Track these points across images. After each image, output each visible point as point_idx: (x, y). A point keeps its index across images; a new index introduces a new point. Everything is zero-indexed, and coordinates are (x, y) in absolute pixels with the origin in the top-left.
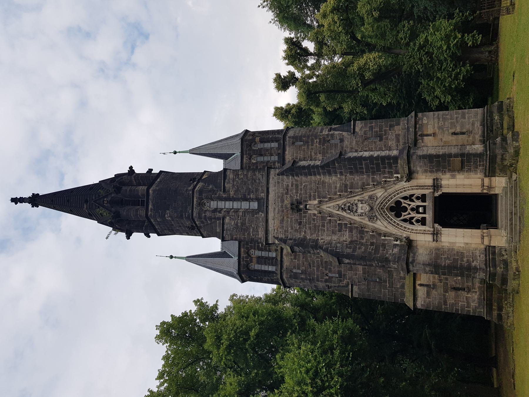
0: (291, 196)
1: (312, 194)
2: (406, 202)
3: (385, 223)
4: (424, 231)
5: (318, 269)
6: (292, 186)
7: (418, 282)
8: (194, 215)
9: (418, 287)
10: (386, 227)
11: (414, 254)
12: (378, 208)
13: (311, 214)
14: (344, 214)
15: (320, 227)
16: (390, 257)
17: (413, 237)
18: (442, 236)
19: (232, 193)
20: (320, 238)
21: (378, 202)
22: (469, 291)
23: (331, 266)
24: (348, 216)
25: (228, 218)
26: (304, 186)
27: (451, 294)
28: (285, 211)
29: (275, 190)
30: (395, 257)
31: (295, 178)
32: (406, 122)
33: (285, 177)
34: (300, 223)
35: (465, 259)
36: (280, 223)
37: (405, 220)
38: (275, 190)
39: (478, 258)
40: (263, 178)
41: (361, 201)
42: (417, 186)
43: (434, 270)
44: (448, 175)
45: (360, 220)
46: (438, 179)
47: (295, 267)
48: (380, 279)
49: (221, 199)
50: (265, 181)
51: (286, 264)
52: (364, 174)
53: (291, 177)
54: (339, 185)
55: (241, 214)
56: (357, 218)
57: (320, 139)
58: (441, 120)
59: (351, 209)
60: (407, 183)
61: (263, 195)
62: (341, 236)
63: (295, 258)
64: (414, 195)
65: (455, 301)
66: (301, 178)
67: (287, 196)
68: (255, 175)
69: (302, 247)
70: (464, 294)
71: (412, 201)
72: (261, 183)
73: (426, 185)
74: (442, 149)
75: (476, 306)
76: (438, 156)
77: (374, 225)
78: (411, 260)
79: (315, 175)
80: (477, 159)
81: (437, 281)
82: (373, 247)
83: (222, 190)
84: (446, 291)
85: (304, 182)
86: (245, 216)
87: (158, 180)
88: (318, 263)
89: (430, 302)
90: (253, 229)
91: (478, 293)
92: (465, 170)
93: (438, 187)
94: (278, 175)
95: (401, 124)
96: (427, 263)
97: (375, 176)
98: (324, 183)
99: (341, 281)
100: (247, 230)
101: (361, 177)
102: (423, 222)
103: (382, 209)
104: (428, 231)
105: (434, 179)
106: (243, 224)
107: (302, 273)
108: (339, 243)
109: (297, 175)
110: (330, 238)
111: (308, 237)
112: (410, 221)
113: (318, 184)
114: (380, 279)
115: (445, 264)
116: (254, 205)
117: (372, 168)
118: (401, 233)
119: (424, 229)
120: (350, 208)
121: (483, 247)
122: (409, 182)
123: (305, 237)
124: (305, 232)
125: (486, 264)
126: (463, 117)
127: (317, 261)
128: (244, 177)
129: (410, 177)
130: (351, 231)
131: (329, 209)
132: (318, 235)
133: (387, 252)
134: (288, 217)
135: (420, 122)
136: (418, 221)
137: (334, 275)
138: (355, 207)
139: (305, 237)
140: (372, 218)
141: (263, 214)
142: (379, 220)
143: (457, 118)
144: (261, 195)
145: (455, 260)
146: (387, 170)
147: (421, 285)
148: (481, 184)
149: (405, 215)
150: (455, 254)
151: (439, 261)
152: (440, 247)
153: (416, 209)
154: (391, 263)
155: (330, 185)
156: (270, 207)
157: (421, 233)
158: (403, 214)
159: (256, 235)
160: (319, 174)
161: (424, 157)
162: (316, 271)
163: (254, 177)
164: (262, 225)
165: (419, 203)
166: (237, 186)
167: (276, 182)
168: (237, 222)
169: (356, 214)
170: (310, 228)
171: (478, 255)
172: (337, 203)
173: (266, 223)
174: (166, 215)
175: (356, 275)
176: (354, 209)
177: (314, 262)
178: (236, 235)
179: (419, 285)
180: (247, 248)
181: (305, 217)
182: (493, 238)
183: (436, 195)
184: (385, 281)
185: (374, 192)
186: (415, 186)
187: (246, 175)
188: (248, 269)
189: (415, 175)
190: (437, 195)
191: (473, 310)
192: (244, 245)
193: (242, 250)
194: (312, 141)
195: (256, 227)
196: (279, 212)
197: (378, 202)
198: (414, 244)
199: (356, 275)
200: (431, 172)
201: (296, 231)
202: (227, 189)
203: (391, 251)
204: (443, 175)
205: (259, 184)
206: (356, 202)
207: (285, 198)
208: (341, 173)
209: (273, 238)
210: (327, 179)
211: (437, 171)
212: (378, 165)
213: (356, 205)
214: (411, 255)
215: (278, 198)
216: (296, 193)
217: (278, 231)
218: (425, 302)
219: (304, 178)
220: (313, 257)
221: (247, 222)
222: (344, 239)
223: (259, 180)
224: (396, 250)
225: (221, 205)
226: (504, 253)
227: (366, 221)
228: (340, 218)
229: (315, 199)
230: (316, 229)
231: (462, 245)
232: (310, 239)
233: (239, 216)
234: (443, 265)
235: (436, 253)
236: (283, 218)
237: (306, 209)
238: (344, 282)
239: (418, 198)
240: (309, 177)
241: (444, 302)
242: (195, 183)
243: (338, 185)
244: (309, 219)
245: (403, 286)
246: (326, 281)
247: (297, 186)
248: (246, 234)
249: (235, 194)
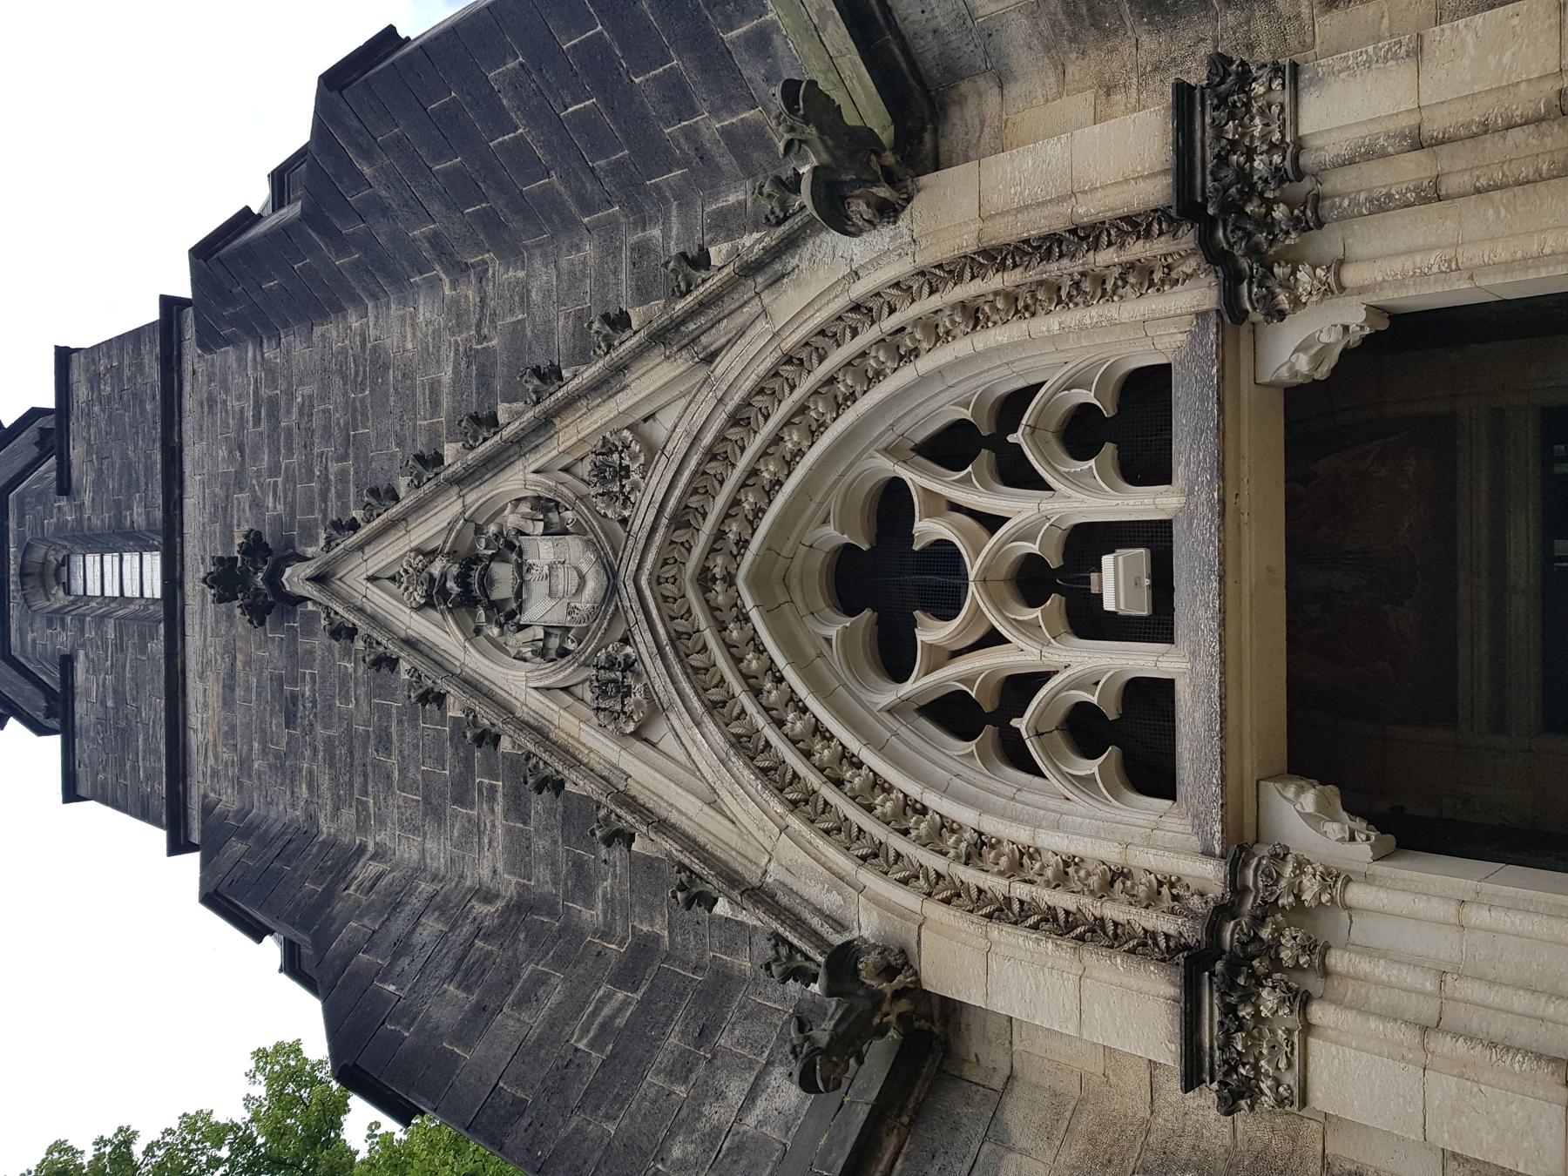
2: (947, 486)
4: (1114, 878)
12: (656, 581)
18: (1317, 1012)
46: (1245, 78)
54: (450, 370)
60: (880, 238)
71: (1018, 474)
73: (1088, 209)
82: (626, 1003)
97: (656, 232)
103: (705, 579)
104: (1165, 891)
105: (1184, 98)
119: (1103, 851)
122: (887, 211)
138: (503, 573)
157: (1050, 915)
158: (931, 633)
169: (516, 640)
190: (1303, 364)
198: (985, 1054)
203: (735, 1091)
243: (447, 375)
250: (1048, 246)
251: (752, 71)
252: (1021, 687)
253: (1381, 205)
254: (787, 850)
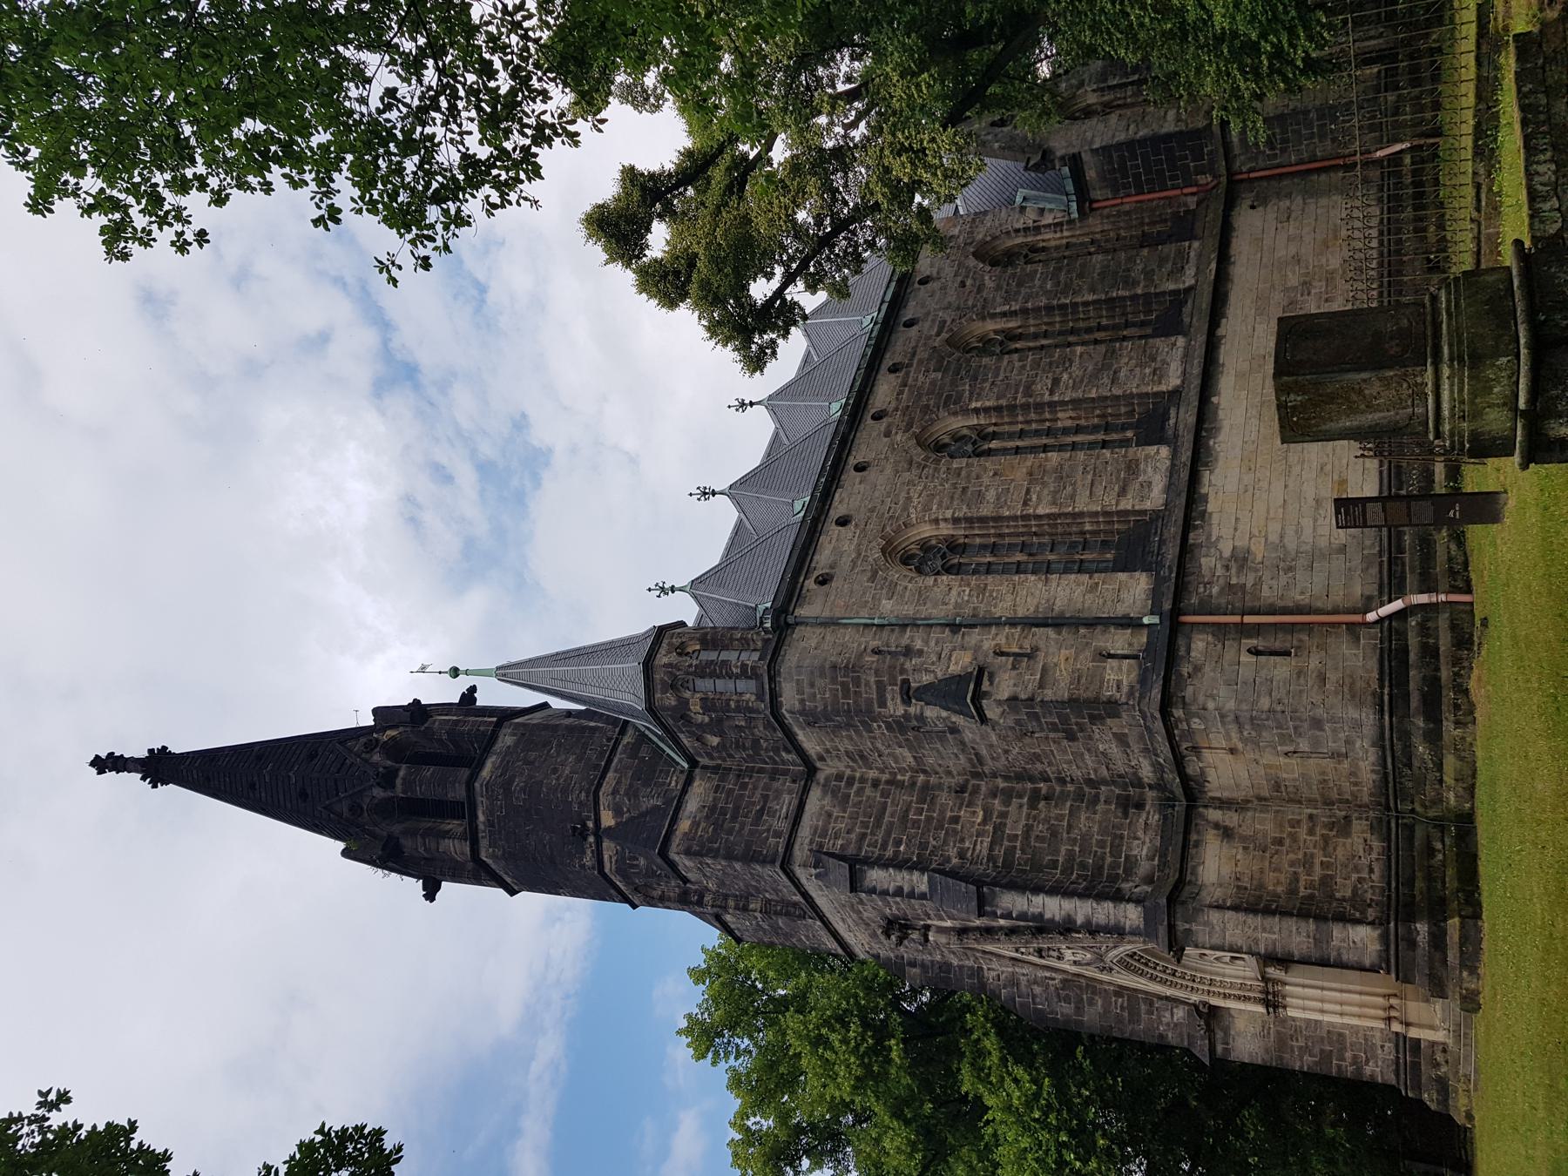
11: (1226, 1031)
16: (1170, 1035)
30: (1181, 1035)
74: (1264, 930)
87: (481, 818)
115: (1302, 1067)
133: (1159, 1017)
145: (1326, 1057)
150: (1322, 1038)
151: (1287, 1056)
171: (1379, 1043)
203: (1168, 1014)
214: (1219, 1035)
235: (1278, 1032)
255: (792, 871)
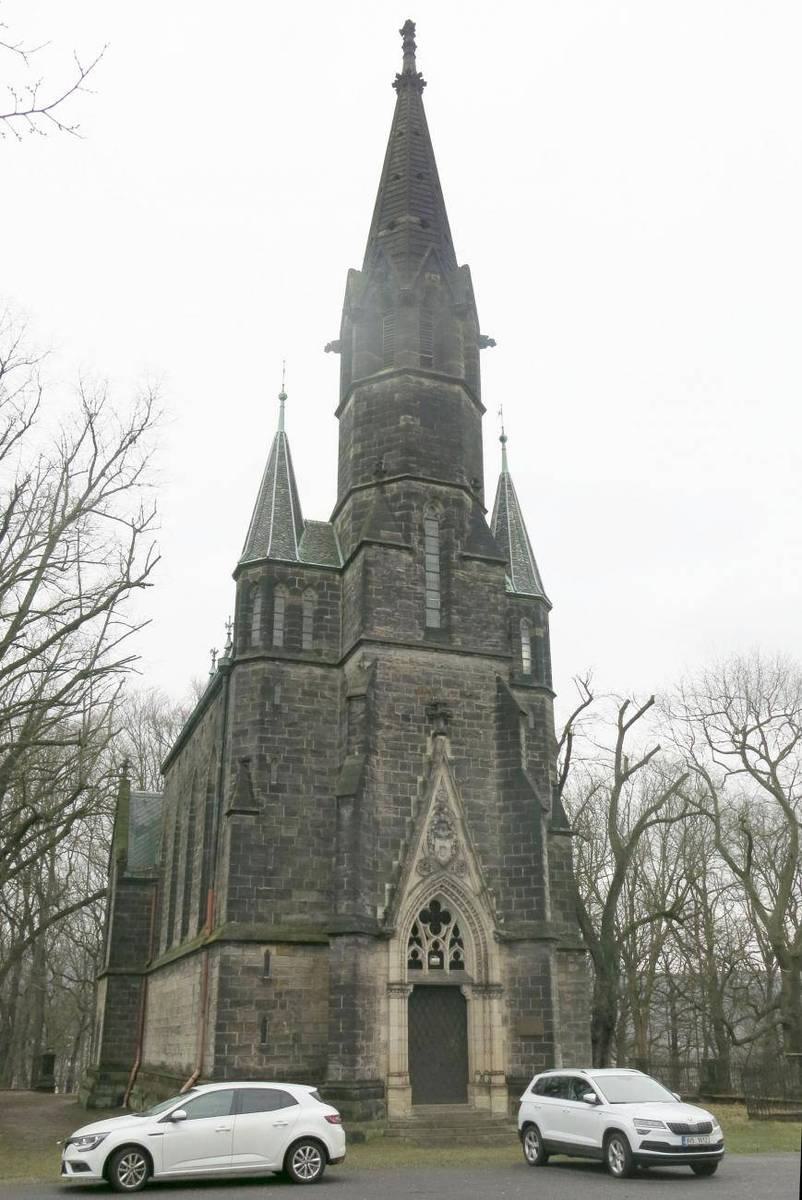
0: (458, 702)
1: (464, 748)
3: (418, 892)
5: (286, 741)
6: (478, 707)
7: (273, 950)
8: (413, 482)
9: (263, 949)
10: (410, 894)
11: (367, 947)
13: (426, 742)
14: (431, 813)
15: (400, 761)
17: (394, 945)
19: (459, 574)
20: (378, 758)
21: (454, 878)
22: (262, 1050)
23: (293, 772)
24: (428, 821)
25: (411, 559)
26: (478, 733)
27: (254, 1016)
28: (429, 688)
29: (468, 668)
31: (493, 714)
32: (570, 932)
33: (494, 693)
34: (406, 718)
35: (364, 1043)
36: (405, 676)
37: (415, 930)
38: (468, 668)
39: (367, 1068)
40: (491, 645)
41: (456, 847)
42: (486, 954)
43: (342, 983)
44: (507, 1011)
45: (421, 842)
47: (285, 690)
48: (272, 873)
49: (445, 547)
50: (486, 650)
51: (292, 670)
52: (505, 853)
53: (493, 705)
55: (419, 589)
56: (424, 837)
57: (539, 764)
58: (575, 997)
59: (442, 825)
60: (492, 936)
61: (458, 642)
62: (386, 802)
63: (304, 693)
64: (462, 947)
65: (241, 1024)
66: (492, 728)
67: (456, 693)
68: (496, 628)
69: (363, 720)
70: (256, 1041)
71: (452, 944)
72: (482, 641)
73: (490, 971)
75: (233, 1064)
76: (547, 993)
77: (414, 870)
78: (360, 940)
79: (499, 756)
80: (542, 1062)
81: (278, 987)
83: (465, 554)
84: (260, 1005)
85: (485, 733)
86: (416, 598)
88: (298, 744)
89: (237, 974)
90: (388, 614)
91: (259, 1067)
92: (516, 1040)
93: (483, 992)
94: (498, 680)
95: (566, 924)
96: (358, 972)
97: (499, 876)
98: (485, 773)
99: (264, 789)
100: (390, 602)
101: (498, 848)
102: (415, 964)
105: (499, 985)
106: (399, 591)
107: (273, 705)
108: (374, 799)
109: (498, 719)
110: (381, 778)
111: (380, 733)
112: (415, 939)
113: (482, 761)
114: (272, 873)
116: (434, 621)
117: (518, 871)
118: (402, 923)
120: (445, 825)
121: (382, 1075)
122: (495, 939)
123: (379, 726)
124: (389, 728)
125: (359, 1082)
126: (580, 1037)
127: (302, 742)
128: (493, 604)
129: (506, 942)
130: (399, 823)
131: (439, 782)
132: (384, 754)
134: (416, 692)
135: (571, 959)
136: (415, 954)
137: (274, 774)
138: (447, 833)
139: (379, 726)
140: (425, 865)
141: (419, 639)
142: (422, 881)
143: (577, 1026)
144: (458, 639)
145: (362, 1023)
146: (514, 899)
147: (267, 956)
148: (494, 1069)
149: (424, 929)
152: (378, 996)
153: (436, 951)
154: (350, 902)
155: (481, 785)
156: (435, 655)
158: (428, 926)
159: (379, 619)
160: (501, 765)
161: (546, 968)
162: (281, 736)
163: (492, 626)
164: (399, 635)
165: (448, 958)
166: (473, 587)
167: (482, 672)
168: (403, 579)
170: (397, 739)
172: (452, 800)
173: (405, 645)
174: (410, 417)
175: (277, 822)
176: (441, 833)
177: (298, 733)
178: (376, 575)
179: (268, 951)
180: (320, 586)
181: (420, 730)
182: (400, 1093)
183: (467, 991)
184: (268, 883)
185: (473, 872)
186: (486, 951)
187: (495, 610)
188: (276, 584)
189: (506, 951)
191: (224, 1059)
192: (327, 579)
193: (318, 574)
194: (538, 748)
195: (394, 622)
196: (427, 673)
197: (454, 878)
198: (380, 947)
199: (277, 822)
200: (512, 980)
201: (392, 709)
202: (468, 563)
204: (507, 1001)
205: (480, 637)
206: (455, 837)
207: (454, 690)
208: (504, 809)
209: (374, 657)
210: (492, 780)
211: (515, 992)
212: (527, 881)
213: (449, 837)
215: (453, 673)
216: (465, 714)
217: (389, 668)
218: (235, 962)
219: (493, 732)
220: (311, 732)
221: (403, 601)
222: (380, 809)
223: (487, 638)
224: (369, 912)
225: (432, 545)
226: (380, 1113)
227: (419, 855)
228: (421, 807)
229: (454, 752)
230: (397, 751)
231: (383, 1037)
232: (376, 737)
233: (415, 584)
234: (357, 1002)
236: (414, 683)
237: (435, 735)
238: (261, 798)
239: (457, 955)
240: (495, 743)
241: (238, 1002)
242: (472, 490)
243: (481, 802)
244: (415, 736)
245: (260, 918)
246: (262, 758)
247: (478, 717)
248: (379, 597)
249: (457, 579)
250: (486, 963)
251: (519, 911)
252: (419, 942)
253: (484, 1007)
254: (405, 912)
255: (503, 661)
